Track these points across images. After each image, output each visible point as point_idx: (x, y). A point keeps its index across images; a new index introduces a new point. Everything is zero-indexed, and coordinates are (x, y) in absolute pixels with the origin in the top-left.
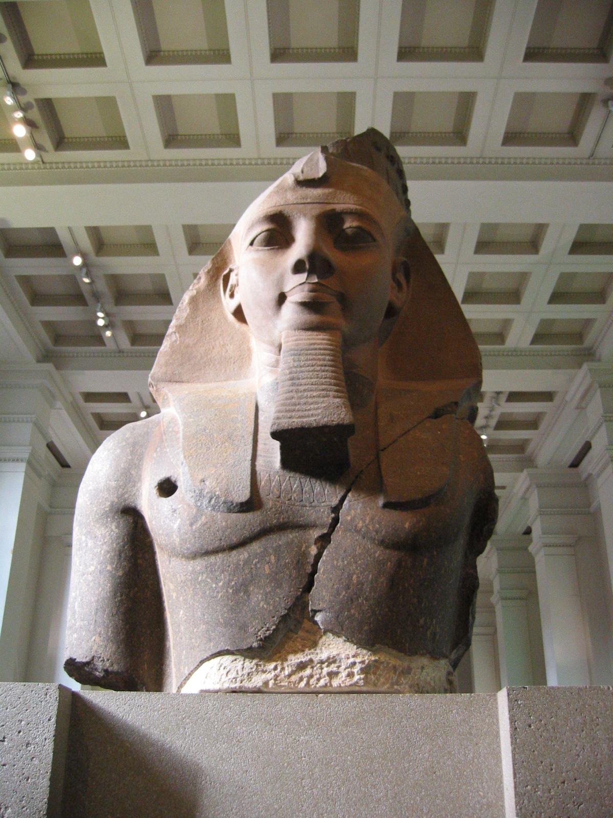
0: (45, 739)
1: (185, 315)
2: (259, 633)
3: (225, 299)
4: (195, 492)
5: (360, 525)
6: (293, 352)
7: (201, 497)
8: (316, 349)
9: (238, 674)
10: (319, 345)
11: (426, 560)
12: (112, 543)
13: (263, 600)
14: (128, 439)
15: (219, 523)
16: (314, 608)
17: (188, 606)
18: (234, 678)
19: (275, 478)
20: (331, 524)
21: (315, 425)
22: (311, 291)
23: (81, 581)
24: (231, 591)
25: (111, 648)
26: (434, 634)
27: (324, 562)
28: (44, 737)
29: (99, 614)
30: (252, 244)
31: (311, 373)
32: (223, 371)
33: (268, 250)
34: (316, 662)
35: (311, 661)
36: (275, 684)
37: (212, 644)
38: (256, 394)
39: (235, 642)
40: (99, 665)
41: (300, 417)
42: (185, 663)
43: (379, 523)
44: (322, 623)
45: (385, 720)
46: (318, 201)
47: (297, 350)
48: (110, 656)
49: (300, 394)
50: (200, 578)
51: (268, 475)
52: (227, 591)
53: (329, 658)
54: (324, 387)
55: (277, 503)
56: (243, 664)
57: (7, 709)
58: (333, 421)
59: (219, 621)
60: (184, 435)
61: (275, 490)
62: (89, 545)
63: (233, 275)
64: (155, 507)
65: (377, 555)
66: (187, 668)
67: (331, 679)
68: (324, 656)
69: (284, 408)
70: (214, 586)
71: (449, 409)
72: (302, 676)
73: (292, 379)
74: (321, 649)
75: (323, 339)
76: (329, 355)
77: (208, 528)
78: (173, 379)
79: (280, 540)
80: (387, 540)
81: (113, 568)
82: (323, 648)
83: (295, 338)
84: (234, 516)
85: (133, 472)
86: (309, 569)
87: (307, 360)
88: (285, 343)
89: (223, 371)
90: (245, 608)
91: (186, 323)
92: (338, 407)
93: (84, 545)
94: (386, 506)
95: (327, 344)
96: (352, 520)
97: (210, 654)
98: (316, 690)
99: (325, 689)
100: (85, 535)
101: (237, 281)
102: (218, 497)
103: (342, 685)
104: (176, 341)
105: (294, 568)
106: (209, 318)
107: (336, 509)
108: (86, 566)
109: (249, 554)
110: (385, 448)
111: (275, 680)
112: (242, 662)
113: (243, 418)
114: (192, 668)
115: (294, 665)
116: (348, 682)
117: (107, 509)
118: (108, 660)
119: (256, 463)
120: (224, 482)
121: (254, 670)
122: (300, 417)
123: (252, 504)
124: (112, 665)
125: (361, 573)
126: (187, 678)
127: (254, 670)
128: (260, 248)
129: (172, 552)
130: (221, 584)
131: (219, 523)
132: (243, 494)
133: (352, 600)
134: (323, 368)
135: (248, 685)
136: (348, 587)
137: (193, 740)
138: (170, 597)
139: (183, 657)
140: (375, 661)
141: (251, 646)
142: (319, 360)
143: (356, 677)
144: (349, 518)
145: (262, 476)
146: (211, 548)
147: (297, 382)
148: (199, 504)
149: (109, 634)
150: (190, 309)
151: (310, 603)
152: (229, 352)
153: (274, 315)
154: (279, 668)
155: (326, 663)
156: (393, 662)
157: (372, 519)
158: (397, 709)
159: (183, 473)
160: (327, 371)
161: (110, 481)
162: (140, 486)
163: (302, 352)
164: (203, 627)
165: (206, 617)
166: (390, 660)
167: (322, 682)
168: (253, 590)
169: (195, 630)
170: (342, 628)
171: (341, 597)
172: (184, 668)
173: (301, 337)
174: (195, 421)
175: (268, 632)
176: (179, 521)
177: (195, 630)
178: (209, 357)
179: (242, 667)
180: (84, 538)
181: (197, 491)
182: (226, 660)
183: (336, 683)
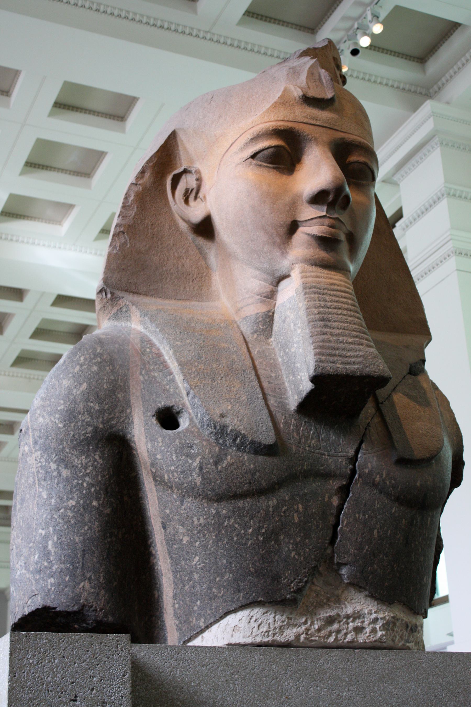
0: (122, 697)
2: (292, 585)
3: (176, 203)
6: (314, 289)
7: (223, 434)
9: (270, 627)
10: (338, 286)
12: (97, 476)
13: (293, 550)
15: (247, 464)
16: (340, 562)
17: (208, 552)
18: (266, 632)
19: (291, 421)
21: (358, 373)
22: (331, 226)
24: (262, 539)
28: (120, 695)
30: (253, 156)
31: (340, 317)
32: (182, 288)
34: (342, 616)
35: (338, 615)
36: (306, 638)
37: (241, 595)
38: (236, 322)
39: (268, 593)
41: (343, 363)
42: (200, 614)
44: (348, 577)
45: (415, 676)
46: (326, 125)
47: (319, 289)
48: (104, 605)
50: (226, 524)
51: (284, 417)
52: (257, 539)
53: (354, 613)
55: (299, 449)
56: (274, 617)
57: (75, 664)
58: (375, 372)
59: (250, 571)
61: (295, 435)
65: (393, 511)
66: (203, 620)
67: (356, 634)
68: (349, 610)
70: (243, 532)
72: (331, 631)
74: (345, 604)
75: (341, 280)
77: (235, 469)
80: (402, 497)
81: (99, 504)
82: (346, 603)
83: (313, 274)
84: (260, 458)
85: (119, 396)
86: (332, 520)
87: (331, 301)
89: (182, 288)
91: (134, 223)
93: (55, 474)
96: (370, 473)
97: (240, 605)
98: (343, 644)
99: (351, 645)
100: (55, 462)
102: (244, 436)
103: (367, 641)
104: (125, 243)
106: (159, 222)
107: (354, 460)
109: (277, 500)
111: (307, 634)
112: (273, 615)
114: (212, 620)
115: (323, 619)
116: (373, 638)
117: (90, 435)
118: (101, 610)
119: (270, 404)
120: (245, 420)
121: (285, 623)
124: (106, 616)
126: (202, 631)
127: (285, 623)
128: (264, 164)
129: (187, 492)
130: (250, 531)
131: (247, 464)
132: (268, 437)
134: (349, 312)
135: (282, 639)
137: (244, 697)
139: (196, 608)
140: (393, 617)
141: (286, 597)
143: (380, 633)
144: (367, 471)
148: (221, 441)
149: (101, 580)
150: (137, 208)
151: (336, 556)
152: (185, 266)
154: (309, 624)
155: (352, 619)
157: (388, 474)
158: (424, 665)
159: (193, 405)
161: (92, 402)
162: (131, 412)
163: (326, 291)
165: (233, 565)
166: (404, 617)
167: (349, 638)
168: (284, 539)
169: (218, 579)
170: (367, 583)
171: (365, 551)
173: (319, 274)
175: (301, 584)
176: (198, 460)
177: (218, 579)
178: (164, 269)
179: (273, 619)
180: (53, 466)
181: (218, 428)
182: (257, 612)
183: (361, 639)
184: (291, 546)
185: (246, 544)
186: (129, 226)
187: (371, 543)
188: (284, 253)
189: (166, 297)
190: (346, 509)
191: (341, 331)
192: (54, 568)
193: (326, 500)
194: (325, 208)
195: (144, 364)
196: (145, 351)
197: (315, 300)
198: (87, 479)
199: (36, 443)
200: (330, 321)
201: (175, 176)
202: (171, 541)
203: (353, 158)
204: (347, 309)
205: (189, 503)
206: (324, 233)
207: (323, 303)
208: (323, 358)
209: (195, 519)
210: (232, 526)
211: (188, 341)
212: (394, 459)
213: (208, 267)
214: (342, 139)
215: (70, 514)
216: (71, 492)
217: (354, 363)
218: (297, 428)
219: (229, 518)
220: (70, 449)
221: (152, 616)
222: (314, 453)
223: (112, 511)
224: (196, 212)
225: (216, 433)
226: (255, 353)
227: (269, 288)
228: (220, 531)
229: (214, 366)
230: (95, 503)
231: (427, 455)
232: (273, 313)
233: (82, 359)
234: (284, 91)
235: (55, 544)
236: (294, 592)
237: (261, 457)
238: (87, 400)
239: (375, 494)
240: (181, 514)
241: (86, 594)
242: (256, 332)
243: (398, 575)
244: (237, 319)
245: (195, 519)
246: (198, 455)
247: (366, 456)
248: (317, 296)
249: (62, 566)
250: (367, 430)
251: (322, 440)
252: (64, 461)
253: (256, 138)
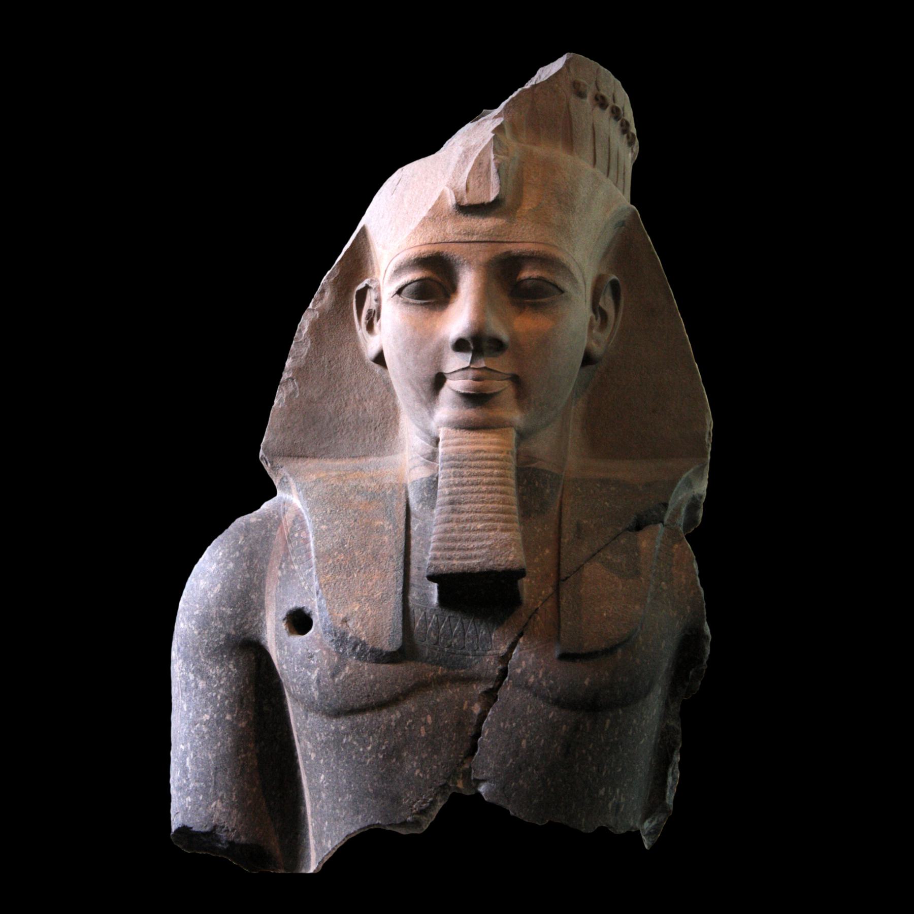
1: (305, 351)
4: (335, 635)
5: (532, 680)
8: (482, 459)
10: (485, 452)
11: (608, 721)
12: (231, 687)
14: (241, 547)
20: (498, 677)
21: (478, 570)
22: (476, 379)
23: (193, 732)
26: (617, 806)
27: (488, 722)
29: (219, 774)
30: (399, 292)
31: (475, 496)
33: (421, 304)
37: (360, 817)
38: (406, 487)
40: (223, 835)
41: (461, 558)
43: (554, 678)
46: (487, 239)
47: (459, 460)
49: (461, 526)
50: (344, 740)
52: (377, 757)
54: (490, 515)
60: (316, 551)
61: (432, 634)
62: (200, 686)
63: (371, 296)
64: (286, 648)
65: (550, 716)
69: (442, 544)
71: (654, 513)
73: (452, 503)
75: (491, 443)
76: (497, 467)
77: (353, 681)
78: (294, 453)
79: (437, 696)
83: (456, 440)
84: (382, 667)
85: (253, 597)
86: (471, 731)
87: (470, 476)
88: (444, 439)
90: (398, 776)
92: (506, 545)
93: (193, 685)
94: (564, 657)
95: (496, 451)
100: (193, 672)
101: (379, 308)
102: (364, 644)
104: (294, 393)
105: (453, 731)
108: (198, 713)
110: (567, 578)
113: (391, 527)
117: (222, 643)
118: (233, 830)
119: (410, 598)
120: (370, 624)
122: (461, 558)
123: (405, 653)
124: (238, 836)
125: (532, 737)
128: (411, 301)
130: (369, 748)
133: (520, 769)
134: (490, 487)
136: (516, 753)
138: (306, 757)
139: (325, 829)
142: (485, 475)
144: (519, 671)
145: (416, 615)
146: (357, 705)
147: (457, 506)
153: (430, 402)
157: (545, 673)
160: (496, 491)
162: (264, 615)
163: (465, 462)
164: (349, 797)
172: (327, 841)
174: (329, 529)
176: (316, 672)
178: (341, 418)
180: (192, 677)
184: (415, 764)
185: (365, 763)
186: (300, 369)
187: (517, 756)
188: (431, 414)
189: (338, 458)
190: (489, 719)
191: (472, 515)
192: (191, 785)
193: (465, 707)
194: (469, 356)
195: (287, 554)
196: (293, 536)
197: (450, 477)
198: (221, 691)
199: (179, 649)
200: (460, 503)
201: (358, 291)
203: (525, 274)
204: (488, 484)
205: (313, 719)
206: (467, 389)
207: (457, 480)
208: (439, 554)
209: (318, 735)
210: (350, 744)
211: (336, 523)
212: (557, 653)
213: (395, 408)
214: (508, 253)
215: (205, 730)
216: (206, 706)
217: (475, 557)
218: (438, 625)
219: (348, 734)
220: (205, 658)
221: (297, 834)
222: (454, 654)
223: (247, 724)
225: (338, 641)
226: (414, 528)
227: (430, 448)
228: (339, 749)
229: (357, 554)
230: (228, 717)
231: (603, 646)
232: (437, 478)
233: (221, 554)
234: (439, 198)
235: (191, 761)
236: (417, 813)
237: (384, 665)
238: (219, 604)
239: (527, 698)
240: (307, 729)
241: (218, 814)
242: (421, 500)
243: (552, 790)
244: (409, 482)
245: (318, 735)
246: (315, 666)
247: (522, 652)
248: (453, 470)
249: (197, 785)
250: (532, 620)
251: (468, 637)
252: (200, 672)
253: (399, 270)
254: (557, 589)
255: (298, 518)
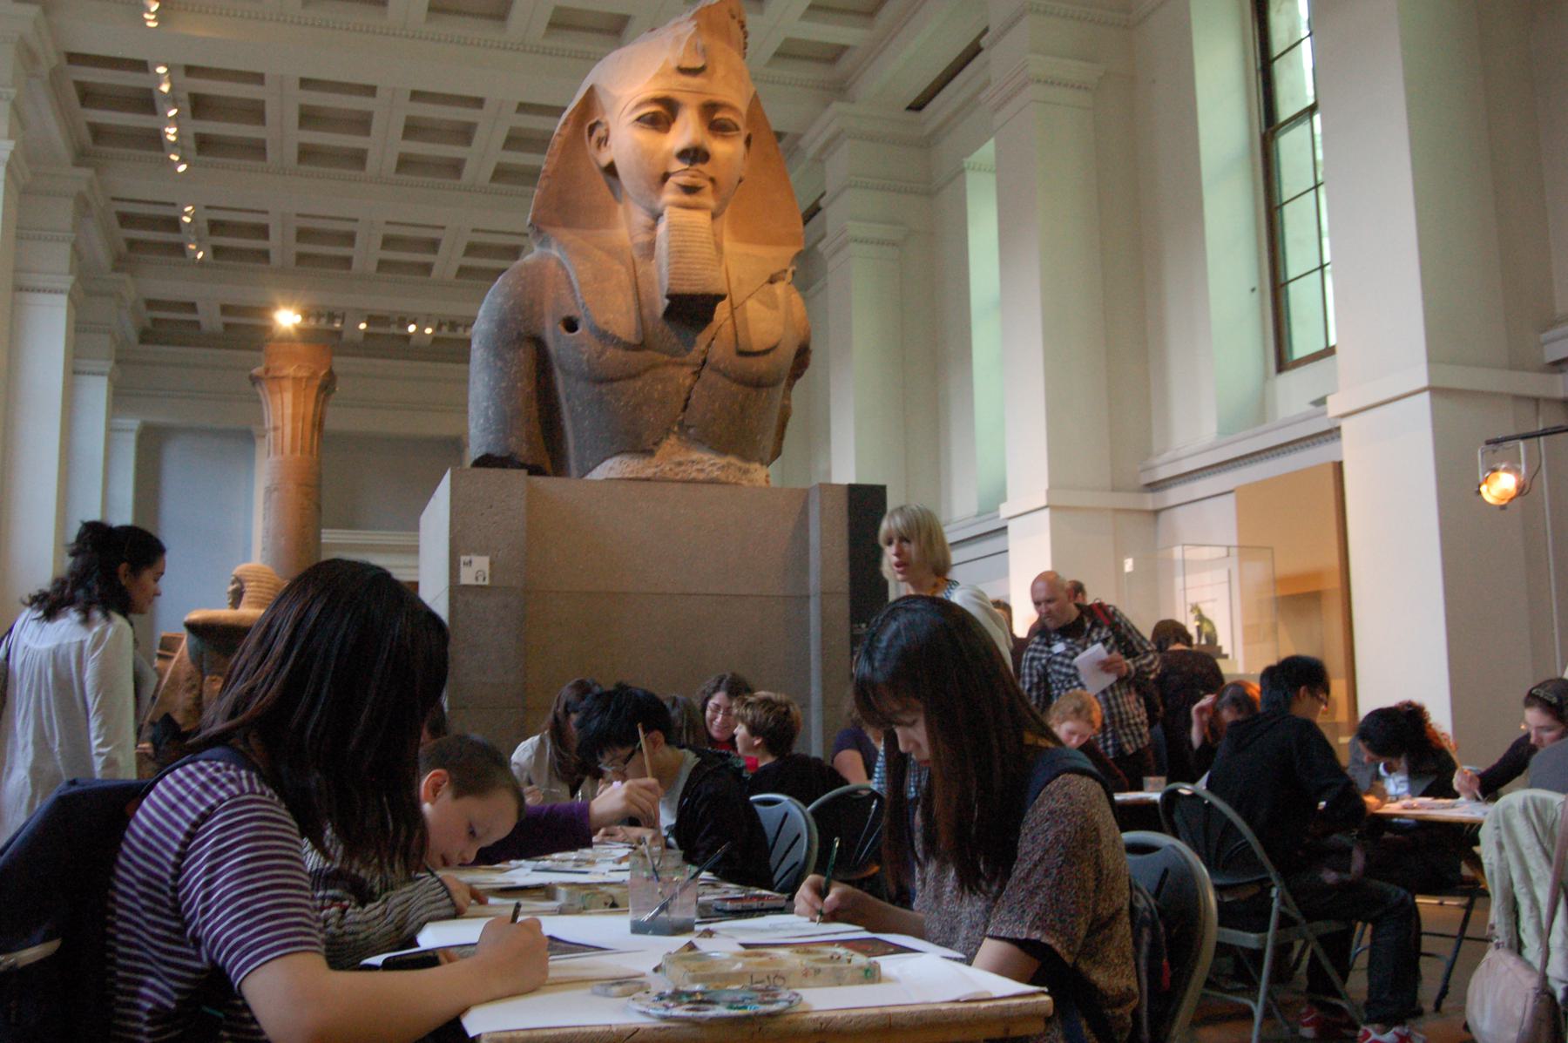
25: (525, 447)
30: (639, 119)
84: (630, 353)
86: (684, 396)
126: (590, 470)
135: (644, 476)
156: (739, 463)
167: (694, 475)
182: (625, 459)
183: (701, 476)
202: (572, 410)
203: (718, 116)
224: (605, 158)
226: (640, 272)
252: (498, 355)
253: (640, 105)
254: (732, 313)
255: (560, 264)
